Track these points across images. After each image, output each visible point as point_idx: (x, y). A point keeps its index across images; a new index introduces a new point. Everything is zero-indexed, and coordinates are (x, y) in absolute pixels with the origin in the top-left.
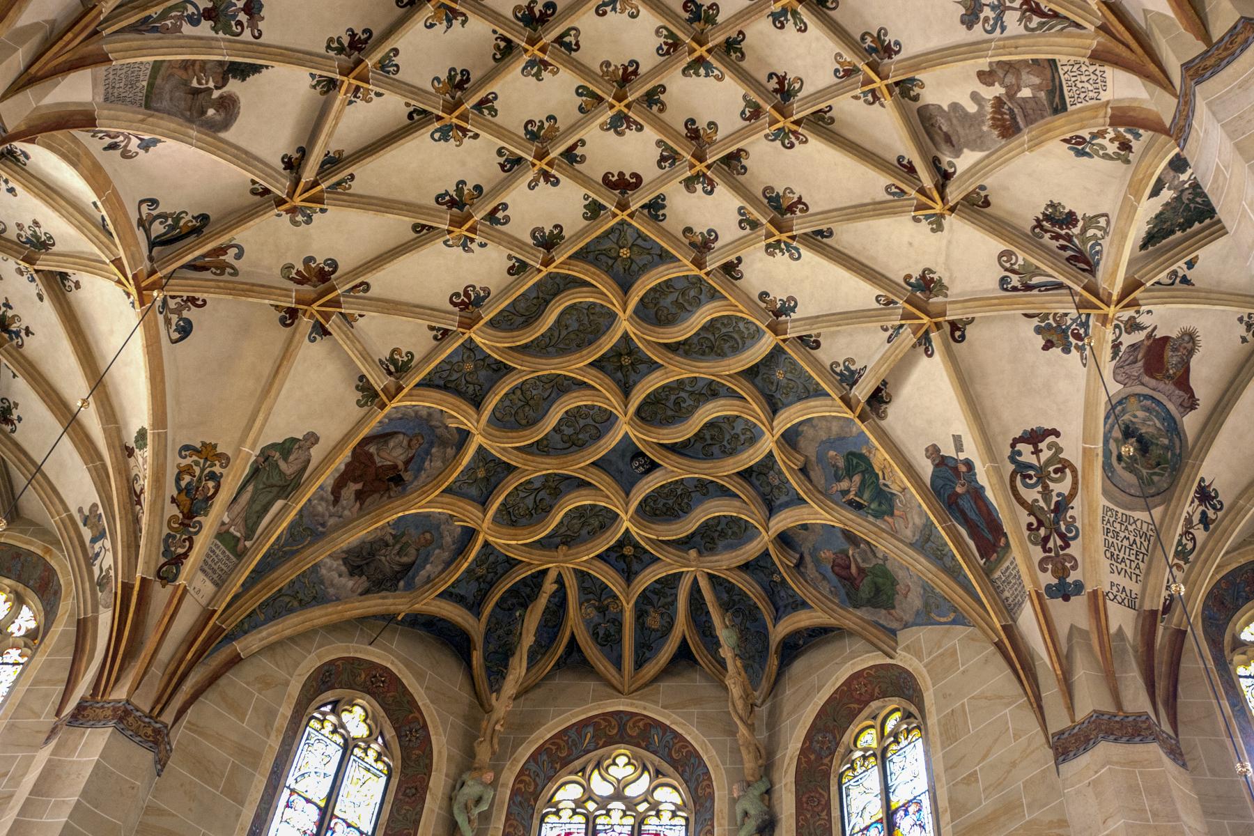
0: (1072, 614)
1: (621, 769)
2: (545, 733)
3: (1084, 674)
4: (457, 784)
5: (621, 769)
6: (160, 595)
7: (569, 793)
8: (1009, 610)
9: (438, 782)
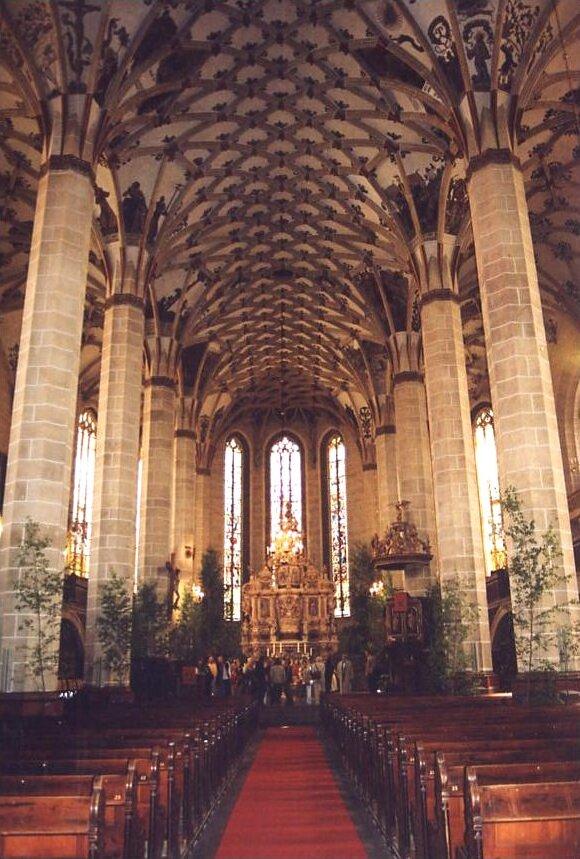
0: (368, 441)
1: (285, 440)
2: (270, 437)
3: (369, 454)
4: (255, 454)
5: (285, 440)
6: (202, 444)
7: (275, 448)
8: (359, 436)
9: (251, 453)
